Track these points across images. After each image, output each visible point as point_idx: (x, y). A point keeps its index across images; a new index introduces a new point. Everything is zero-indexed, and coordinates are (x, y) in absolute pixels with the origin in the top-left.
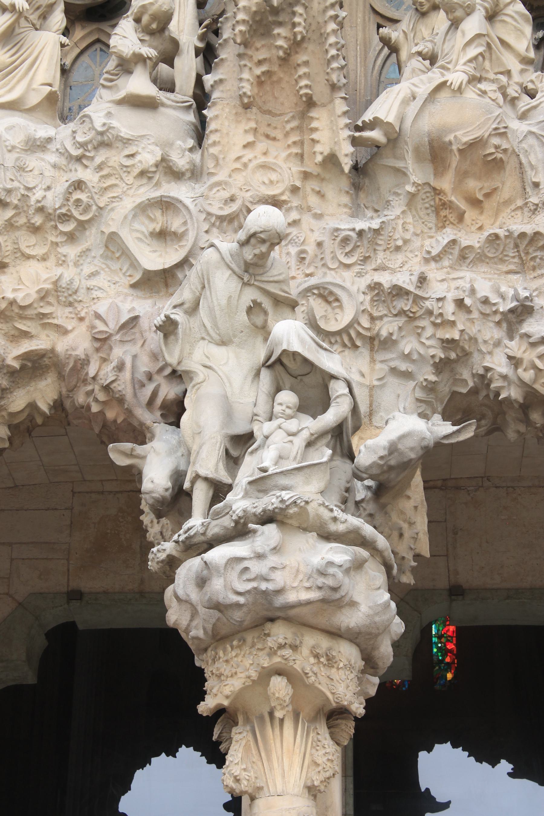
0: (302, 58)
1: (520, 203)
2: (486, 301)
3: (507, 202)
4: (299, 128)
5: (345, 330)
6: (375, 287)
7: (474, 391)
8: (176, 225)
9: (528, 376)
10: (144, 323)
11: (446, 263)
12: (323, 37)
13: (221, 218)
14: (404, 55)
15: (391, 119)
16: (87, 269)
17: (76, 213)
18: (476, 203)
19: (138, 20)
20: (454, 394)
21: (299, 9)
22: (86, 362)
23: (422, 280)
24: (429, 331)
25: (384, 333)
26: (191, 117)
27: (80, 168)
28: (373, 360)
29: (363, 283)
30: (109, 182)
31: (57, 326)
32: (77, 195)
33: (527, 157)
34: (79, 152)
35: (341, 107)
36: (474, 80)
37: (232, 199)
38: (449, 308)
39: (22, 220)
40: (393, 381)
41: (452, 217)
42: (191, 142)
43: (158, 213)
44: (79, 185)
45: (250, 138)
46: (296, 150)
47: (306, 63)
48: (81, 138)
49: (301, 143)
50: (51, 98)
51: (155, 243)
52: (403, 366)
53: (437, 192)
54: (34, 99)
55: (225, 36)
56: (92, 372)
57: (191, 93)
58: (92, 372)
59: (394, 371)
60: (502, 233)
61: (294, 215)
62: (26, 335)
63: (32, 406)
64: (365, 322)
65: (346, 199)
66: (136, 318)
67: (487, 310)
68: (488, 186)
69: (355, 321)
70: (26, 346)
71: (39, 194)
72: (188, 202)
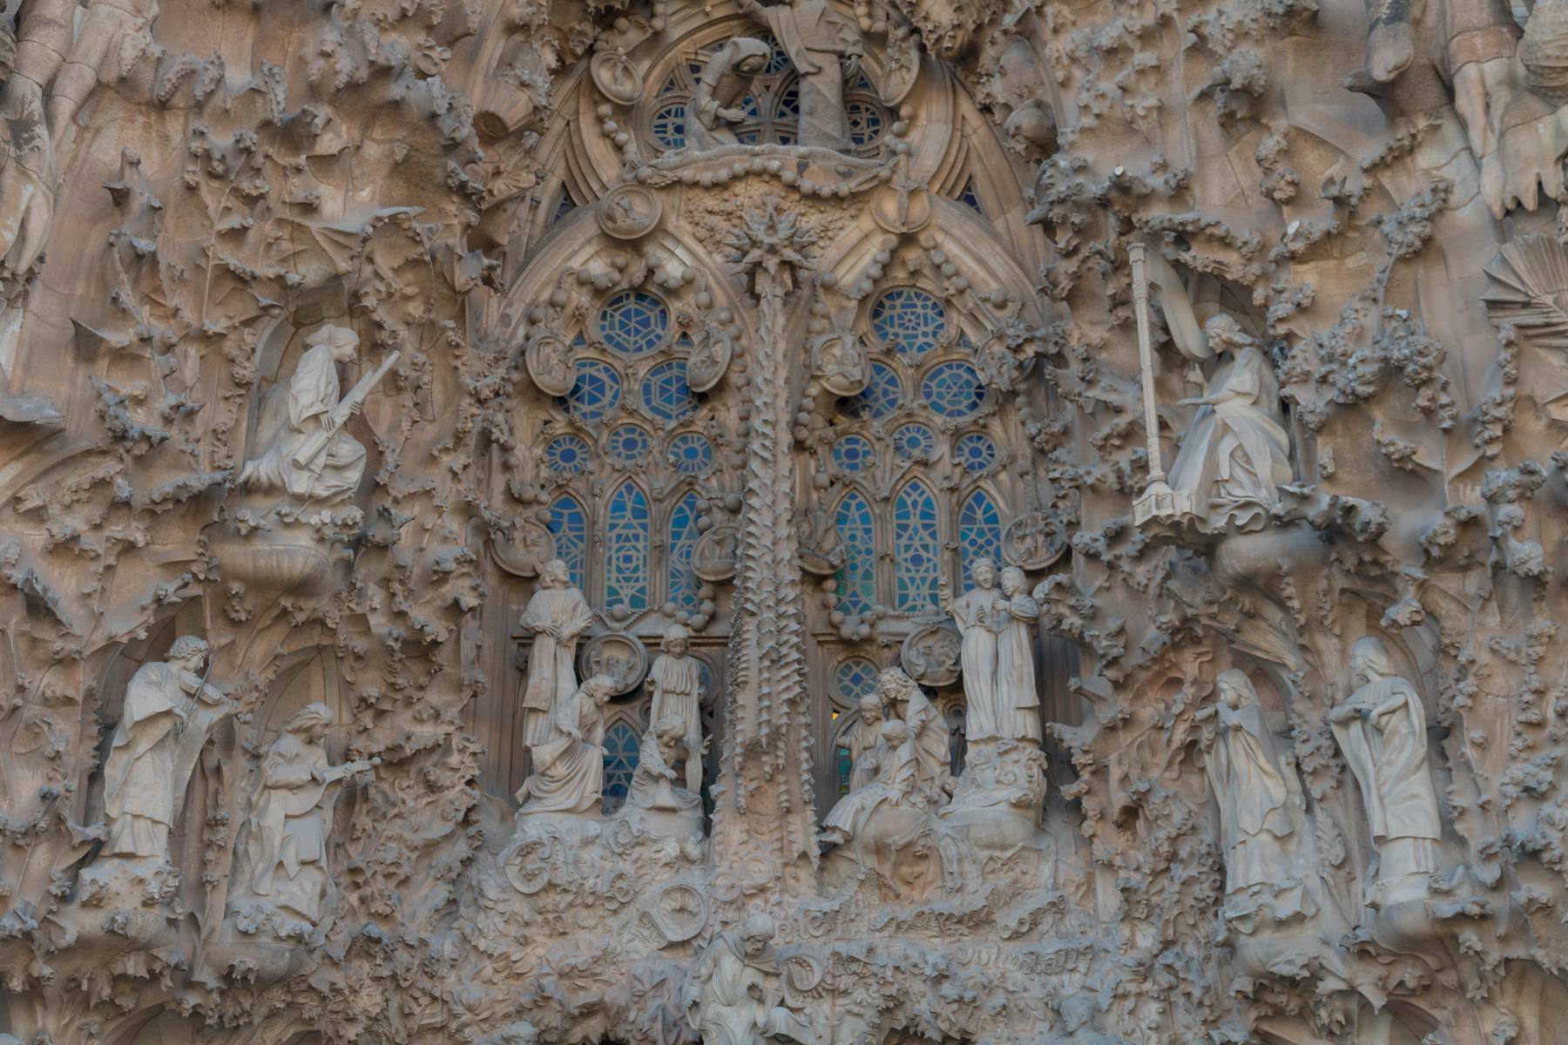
0: (781, 778)
1: (939, 883)
2: (916, 966)
3: (931, 882)
4: (780, 827)
5: (815, 988)
6: (835, 954)
7: (906, 1028)
8: (692, 906)
9: (945, 1026)
10: (671, 984)
11: (886, 933)
12: (797, 763)
13: (725, 903)
14: (854, 754)
15: (847, 828)
16: (626, 937)
17: (619, 897)
18: (909, 883)
19: (660, 737)
20: (893, 1030)
21: (781, 745)
22: (627, 1009)
23: (870, 951)
24: (875, 987)
25: (842, 987)
26: (699, 813)
27: (621, 863)
28: (834, 1005)
29: (827, 951)
30: (642, 872)
31: (605, 982)
32: (620, 884)
33: (945, 849)
34: (620, 850)
35: (812, 818)
36: (906, 794)
37: (733, 887)
38: (889, 973)
39: (579, 901)
40: (848, 1018)
41: (891, 895)
42: (700, 835)
43: (678, 895)
44: (620, 876)
45: (745, 837)
46: (777, 845)
47: (786, 782)
48: (622, 840)
49: (782, 838)
50: (598, 801)
51: (676, 916)
52: (856, 1009)
53: (880, 875)
54: (587, 804)
55: (725, 755)
56: (631, 1018)
57: (698, 789)
58: (631, 1018)
59: (849, 1012)
60: (926, 909)
61: (775, 898)
62: (583, 988)
63: (586, 1037)
64: (829, 980)
65: (813, 882)
66: (663, 981)
67: (916, 971)
68: (917, 869)
69: (823, 980)
70: (582, 998)
71: (589, 883)
72: (700, 889)
